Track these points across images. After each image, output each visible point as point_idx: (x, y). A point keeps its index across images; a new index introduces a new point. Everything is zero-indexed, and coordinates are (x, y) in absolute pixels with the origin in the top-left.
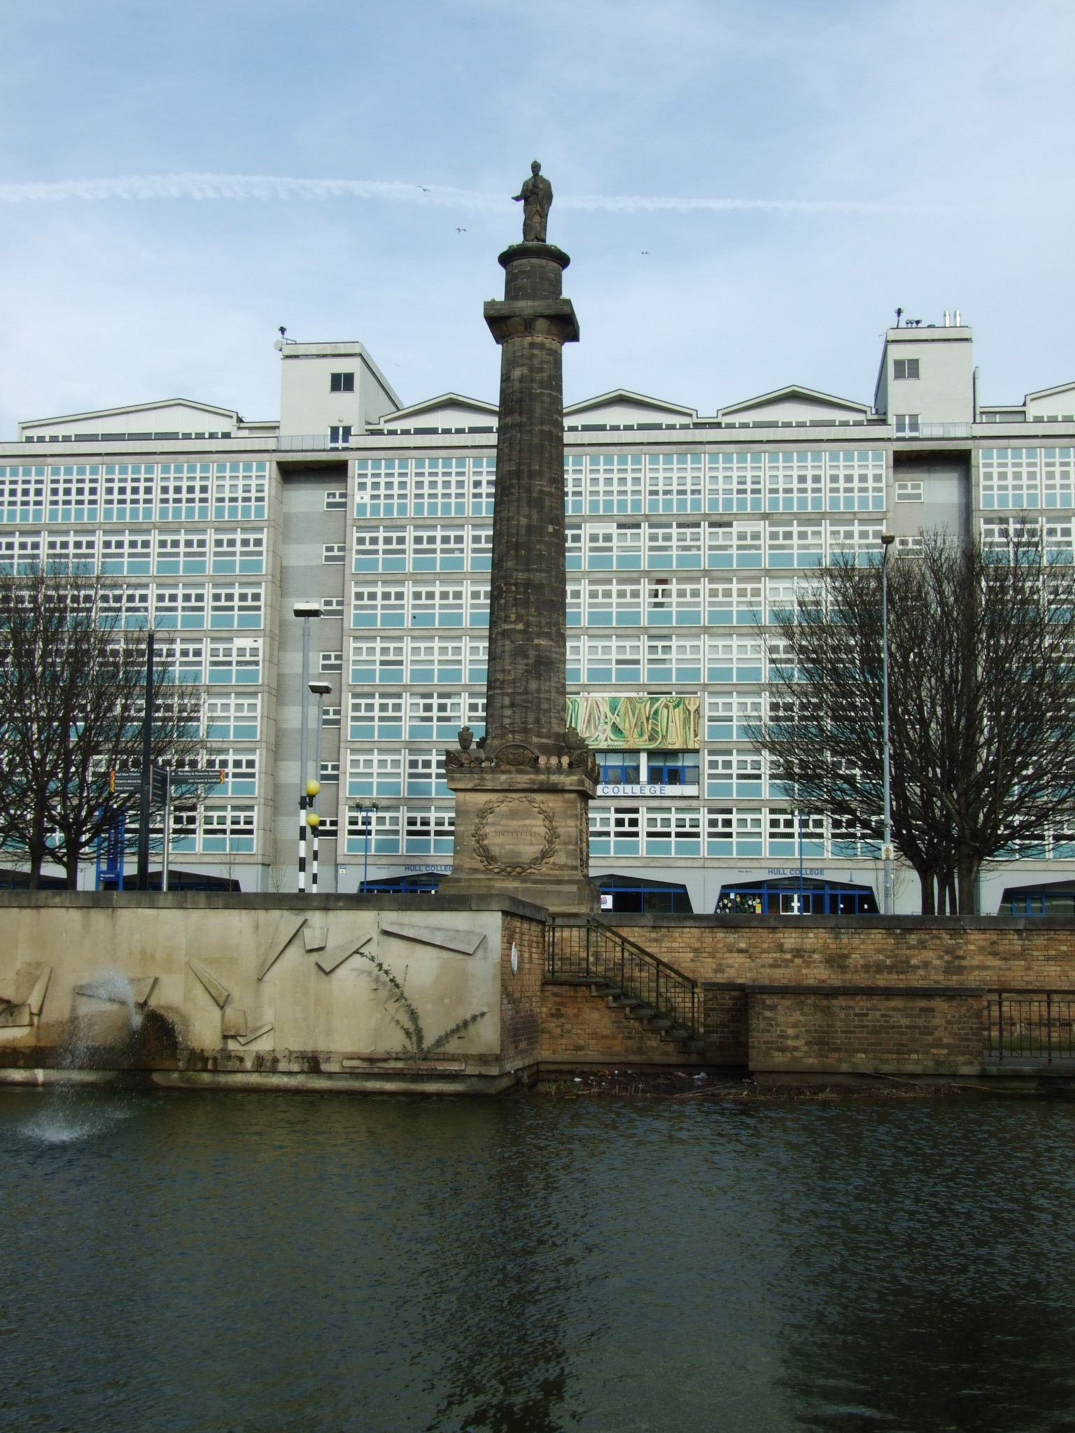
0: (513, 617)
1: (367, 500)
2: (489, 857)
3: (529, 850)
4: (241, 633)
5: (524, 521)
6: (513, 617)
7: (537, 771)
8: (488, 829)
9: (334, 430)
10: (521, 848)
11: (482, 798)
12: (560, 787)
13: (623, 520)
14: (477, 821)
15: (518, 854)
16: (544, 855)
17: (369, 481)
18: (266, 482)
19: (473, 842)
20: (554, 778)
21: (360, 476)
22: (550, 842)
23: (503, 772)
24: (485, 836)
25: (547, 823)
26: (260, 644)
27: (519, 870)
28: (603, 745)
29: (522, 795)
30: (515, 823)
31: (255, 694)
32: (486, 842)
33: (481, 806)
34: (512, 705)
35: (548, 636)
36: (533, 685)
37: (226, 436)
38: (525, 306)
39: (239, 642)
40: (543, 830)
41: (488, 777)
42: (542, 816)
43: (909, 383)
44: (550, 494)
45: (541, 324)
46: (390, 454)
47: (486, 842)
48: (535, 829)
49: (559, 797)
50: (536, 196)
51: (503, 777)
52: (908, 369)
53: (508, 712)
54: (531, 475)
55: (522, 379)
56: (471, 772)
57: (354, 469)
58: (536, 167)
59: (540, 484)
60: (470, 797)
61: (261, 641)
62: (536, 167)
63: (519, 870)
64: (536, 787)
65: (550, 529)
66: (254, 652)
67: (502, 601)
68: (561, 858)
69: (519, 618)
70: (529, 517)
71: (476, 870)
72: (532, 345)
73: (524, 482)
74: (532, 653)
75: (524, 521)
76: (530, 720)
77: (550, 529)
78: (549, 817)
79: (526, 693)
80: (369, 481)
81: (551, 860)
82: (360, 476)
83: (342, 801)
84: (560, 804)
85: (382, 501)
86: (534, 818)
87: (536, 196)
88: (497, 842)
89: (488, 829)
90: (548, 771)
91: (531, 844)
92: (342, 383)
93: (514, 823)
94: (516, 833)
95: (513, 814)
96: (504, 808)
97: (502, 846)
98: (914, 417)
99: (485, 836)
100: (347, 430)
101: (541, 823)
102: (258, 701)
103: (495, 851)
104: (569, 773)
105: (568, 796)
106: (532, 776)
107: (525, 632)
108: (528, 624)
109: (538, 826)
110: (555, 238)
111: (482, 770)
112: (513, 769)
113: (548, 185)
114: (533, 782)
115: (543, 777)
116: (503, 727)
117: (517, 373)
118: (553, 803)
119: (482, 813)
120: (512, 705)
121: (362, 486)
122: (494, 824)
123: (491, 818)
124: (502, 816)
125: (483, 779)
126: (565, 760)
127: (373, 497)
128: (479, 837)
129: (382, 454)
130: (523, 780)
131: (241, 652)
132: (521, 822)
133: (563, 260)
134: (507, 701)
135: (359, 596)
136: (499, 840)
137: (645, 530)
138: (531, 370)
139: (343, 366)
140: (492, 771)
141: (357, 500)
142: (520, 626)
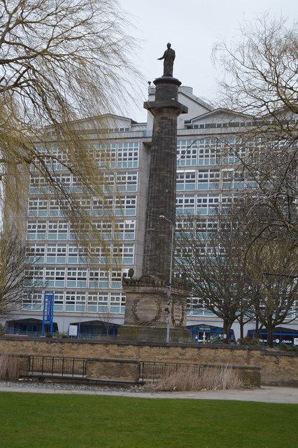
2: (136, 318)
3: (151, 316)
4: (128, 218)
5: (157, 188)
10: (148, 315)
11: (134, 297)
16: (157, 318)
18: (138, 151)
19: (131, 313)
23: (143, 286)
26: (134, 223)
31: (132, 245)
35: (164, 233)
36: (158, 252)
37: (127, 129)
38: (160, 104)
40: (156, 309)
44: (167, 177)
46: (189, 138)
50: (169, 57)
51: (142, 288)
54: (160, 170)
56: (131, 286)
58: (169, 45)
59: (163, 173)
60: (130, 295)
61: (135, 221)
62: (169, 45)
65: (167, 191)
66: (132, 226)
70: (159, 186)
72: (163, 118)
73: (158, 172)
75: (157, 188)
77: (167, 191)
85: (186, 159)
87: (169, 57)
88: (139, 313)
93: (146, 306)
94: (145, 310)
95: (146, 302)
96: (143, 300)
102: (133, 248)
109: (154, 306)
110: (176, 75)
111: (135, 286)
113: (173, 52)
117: (157, 129)
128: (134, 311)
129: (186, 138)
130: (149, 289)
133: (179, 83)
138: (162, 128)
140: (138, 286)
142: (153, 229)
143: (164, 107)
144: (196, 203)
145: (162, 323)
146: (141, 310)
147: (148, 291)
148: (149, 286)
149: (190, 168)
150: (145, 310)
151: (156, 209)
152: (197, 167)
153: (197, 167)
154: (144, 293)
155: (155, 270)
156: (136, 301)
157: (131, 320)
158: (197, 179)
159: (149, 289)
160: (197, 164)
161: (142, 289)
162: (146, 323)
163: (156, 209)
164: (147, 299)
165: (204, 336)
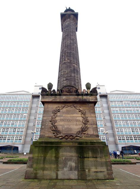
0: (66, 59)
2: (56, 131)
3: (76, 128)
4: (24, 114)
6: (66, 59)
10: (72, 127)
11: (54, 107)
12: (88, 100)
14: (52, 115)
15: (71, 129)
16: (83, 130)
19: (50, 124)
22: (85, 124)
27: (71, 137)
29: (72, 104)
30: (69, 115)
32: (56, 124)
33: (54, 109)
34: (66, 80)
39: (24, 115)
40: (81, 119)
41: (58, 97)
42: (80, 113)
47: (56, 124)
48: (78, 118)
51: (64, 97)
53: (65, 82)
63: (71, 137)
64: (78, 100)
68: (91, 132)
74: (72, 67)
79: (71, 76)
81: (86, 132)
86: (77, 114)
89: (57, 118)
91: (76, 125)
93: (69, 116)
95: (68, 112)
96: (65, 110)
97: (63, 126)
101: (80, 115)
103: (60, 128)
104: (91, 95)
106: (76, 97)
107: (70, 62)
109: (79, 117)
115: (80, 97)
120: (66, 80)
123: (58, 114)
124: (63, 113)
128: (53, 122)
131: (24, 116)
132: (72, 115)
134: (65, 79)
136: (62, 123)
142: (69, 61)
145: (91, 136)
159: (72, 98)
162: (69, 137)
164: (69, 108)
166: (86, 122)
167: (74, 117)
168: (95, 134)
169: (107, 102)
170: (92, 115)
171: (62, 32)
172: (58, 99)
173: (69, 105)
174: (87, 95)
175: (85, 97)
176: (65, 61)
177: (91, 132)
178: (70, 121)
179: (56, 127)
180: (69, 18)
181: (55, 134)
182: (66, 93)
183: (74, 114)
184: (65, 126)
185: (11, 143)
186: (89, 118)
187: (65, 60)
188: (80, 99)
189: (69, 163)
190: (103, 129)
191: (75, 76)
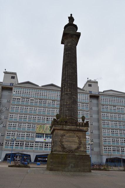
0: (68, 90)
1: (15, 93)
2: (63, 148)
3: (74, 146)
5: (71, 71)
6: (68, 90)
7: (77, 126)
8: (64, 140)
9: (11, 84)
11: (62, 132)
13: (53, 100)
14: (61, 138)
16: (78, 148)
17: (16, 91)
19: (59, 143)
20: (81, 128)
21: (14, 90)
24: (63, 142)
25: (79, 139)
28: (48, 133)
30: (70, 139)
32: (63, 144)
34: (68, 110)
40: (77, 141)
43: (90, 87)
45: (75, 37)
47: (63, 144)
48: (76, 141)
49: (81, 133)
52: (90, 85)
53: (67, 112)
55: (70, 45)
56: (60, 125)
57: (14, 89)
58: (71, 15)
62: (71, 15)
67: (66, 87)
68: (82, 149)
69: (70, 91)
71: (60, 151)
72: (72, 40)
74: (73, 99)
75: (71, 71)
76: (72, 114)
78: (79, 138)
79: (71, 107)
80: (16, 91)
81: (80, 149)
82: (14, 90)
83: (5, 140)
84: (82, 135)
86: (75, 138)
88: (66, 144)
89: (64, 140)
90: (80, 126)
91: (75, 145)
92: (13, 78)
93: (71, 139)
94: (70, 142)
95: (70, 137)
96: (68, 135)
98: (91, 92)
99: (63, 142)
100: (13, 84)
101: (77, 139)
103: (65, 146)
104: (85, 126)
105: (84, 133)
106: (75, 127)
107: (71, 94)
108: (72, 92)
109: (76, 140)
111: (63, 125)
112: (71, 124)
114: (76, 128)
115: (78, 127)
116: (66, 115)
118: (80, 134)
119: (63, 136)
121: (14, 91)
122: (65, 139)
123: (64, 137)
125: (63, 127)
126: (84, 124)
127: (16, 93)
128: (61, 142)
130: (73, 127)
132: (72, 139)
134: (67, 109)
135: (12, 107)
136: (66, 143)
137: (56, 102)
139: (13, 75)
140: (66, 125)
141: (13, 93)
142: (70, 93)
143: (75, 35)
144: (20, 108)
145: (83, 151)
146: (66, 141)
147: (73, 129)
148: (74, 126)
149: (18, 97)
150: (70, 142)
151: (71, 82)
152: (21, 97)
153: (21, 97)
154: (69, 130)
155: (72, 116)
156: (63, 136)
157: (58, 148)
158: (21, 100)
159: (73, 127)
160: (21, 96)
161: (68, 127)
162: (71, 151)
163: (71, 82)
164: (71, 134)
165: (18, 157)
166: (80, 143)
167: (73, 140)
168: (84, 150)
169: (98, 105)
170: (85, 140)
171: (62, 43)
172: (65, 127)
173: (71, 132)
174: (82, 126)
175: (81, 128)
176: (68, 92)
177: (82, 149)
178: (71, 142)
179: (63, 145)
180: (71, 35)
181: (63, 149)
182: (69, 124)
183: (74, 138)
184: (69, 145)
185: (21, 151)
186: (82, 141)
187: (67, 91)
188: (78, 129)
189: (71, 164)
190: (89, 137)
191: (74, 107)
